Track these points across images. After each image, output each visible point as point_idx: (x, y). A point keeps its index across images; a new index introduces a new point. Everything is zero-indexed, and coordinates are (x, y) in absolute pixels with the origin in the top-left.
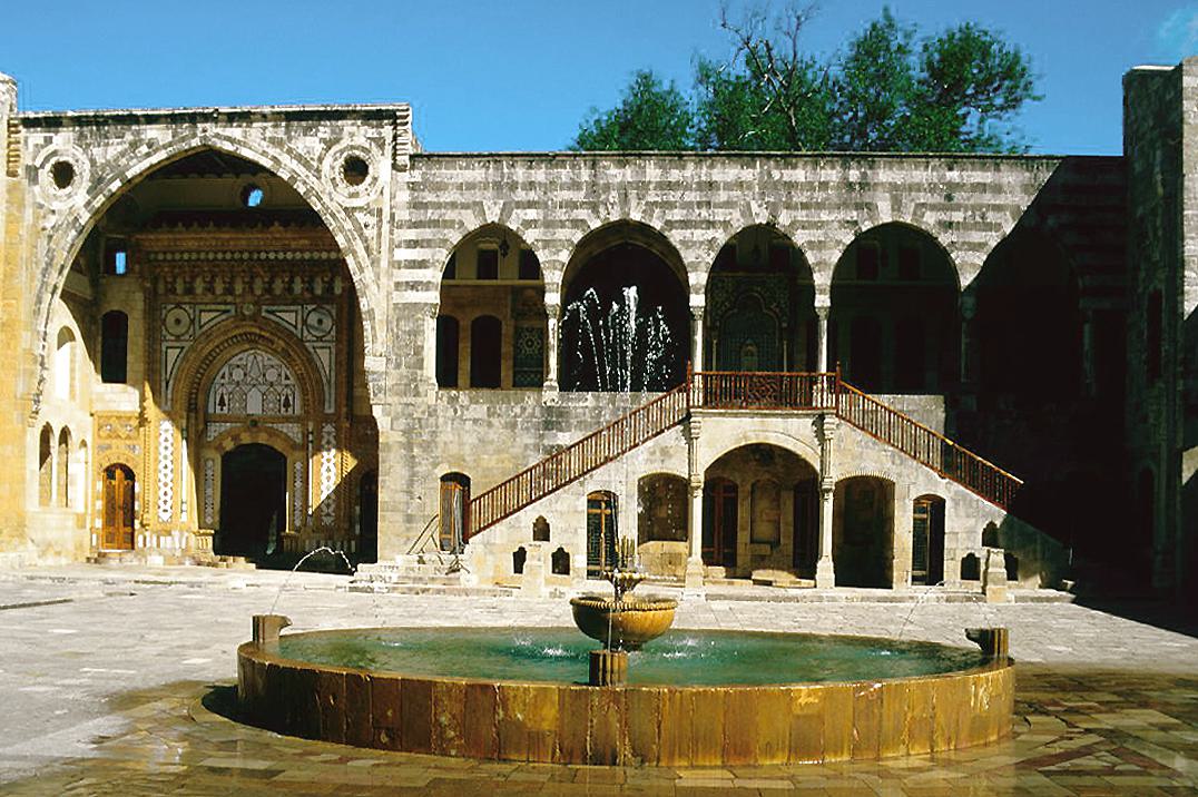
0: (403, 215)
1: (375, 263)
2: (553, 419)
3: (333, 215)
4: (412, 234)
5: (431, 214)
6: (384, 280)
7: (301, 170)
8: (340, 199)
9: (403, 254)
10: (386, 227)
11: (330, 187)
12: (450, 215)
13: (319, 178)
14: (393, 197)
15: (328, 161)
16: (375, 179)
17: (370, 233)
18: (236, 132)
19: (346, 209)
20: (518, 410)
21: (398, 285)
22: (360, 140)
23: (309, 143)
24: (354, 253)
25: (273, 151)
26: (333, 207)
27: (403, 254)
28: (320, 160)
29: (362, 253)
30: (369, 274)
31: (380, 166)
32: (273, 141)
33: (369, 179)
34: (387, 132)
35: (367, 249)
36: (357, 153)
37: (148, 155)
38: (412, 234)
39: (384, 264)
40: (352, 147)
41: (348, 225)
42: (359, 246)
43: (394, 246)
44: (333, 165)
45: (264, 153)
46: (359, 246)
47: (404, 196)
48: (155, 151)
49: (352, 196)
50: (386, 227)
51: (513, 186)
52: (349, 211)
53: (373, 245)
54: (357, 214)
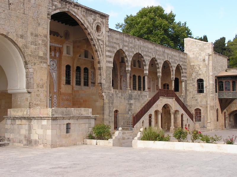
0: (107, 43)
1: (103, 54)
2: (130, 98)
3: (95, 40)
4: (108, 49)
5: (112, 44)
6: (104, 59)
7: (89, 25)
8: (96, 36)
9: (108, 54)
10: (104, 46)
11: (94, 32)
12: (115, 45)
13: (92, 29)
14: (106, 38)
15: (94, 25)
16: (102, 32)
17: (102, 46)
18: (76, 10)
19: (98, 39)
20: (125, 95)
21: (107, 61)
22: (100, 21)
23: (90, 19)
24: (99, 51)
25: (83, 19)
26: (95, 38)
27: (108, 54)
28: (93, 24)
29: (100, 52)
30: (102, 57)
31: (103, 30)
32: (83, 15)
33: (101, 33)
34: (104, 20)
35: (101, 50)
36: (99, 24)
37: (55, 10)
38: (108, 49)
39: (104, 55)
40: (98, 23)
41: (98, 44)
42: (100, 50)
43: (106, 51)
44: (94, 26)
45: (81, 19)
46: (100, 50)
47: (107, 38)
48: (57, 9)
49: (99, 36)
50: (104, 46)
51: (124, 41)
52: (98, 40)
53: (102, 50)
54: (100, 41)
